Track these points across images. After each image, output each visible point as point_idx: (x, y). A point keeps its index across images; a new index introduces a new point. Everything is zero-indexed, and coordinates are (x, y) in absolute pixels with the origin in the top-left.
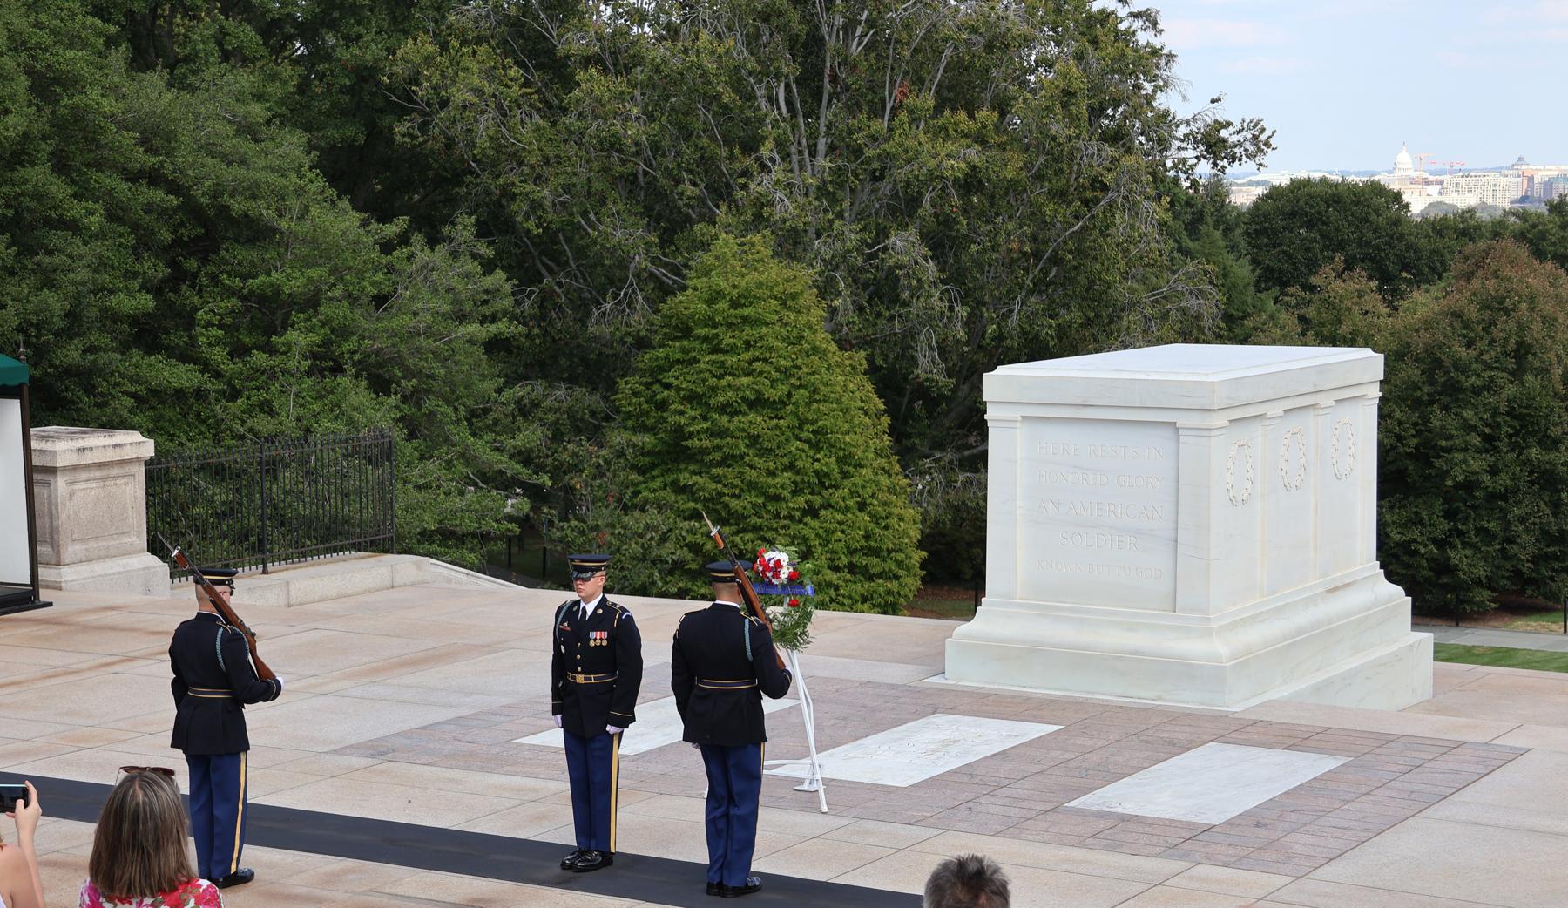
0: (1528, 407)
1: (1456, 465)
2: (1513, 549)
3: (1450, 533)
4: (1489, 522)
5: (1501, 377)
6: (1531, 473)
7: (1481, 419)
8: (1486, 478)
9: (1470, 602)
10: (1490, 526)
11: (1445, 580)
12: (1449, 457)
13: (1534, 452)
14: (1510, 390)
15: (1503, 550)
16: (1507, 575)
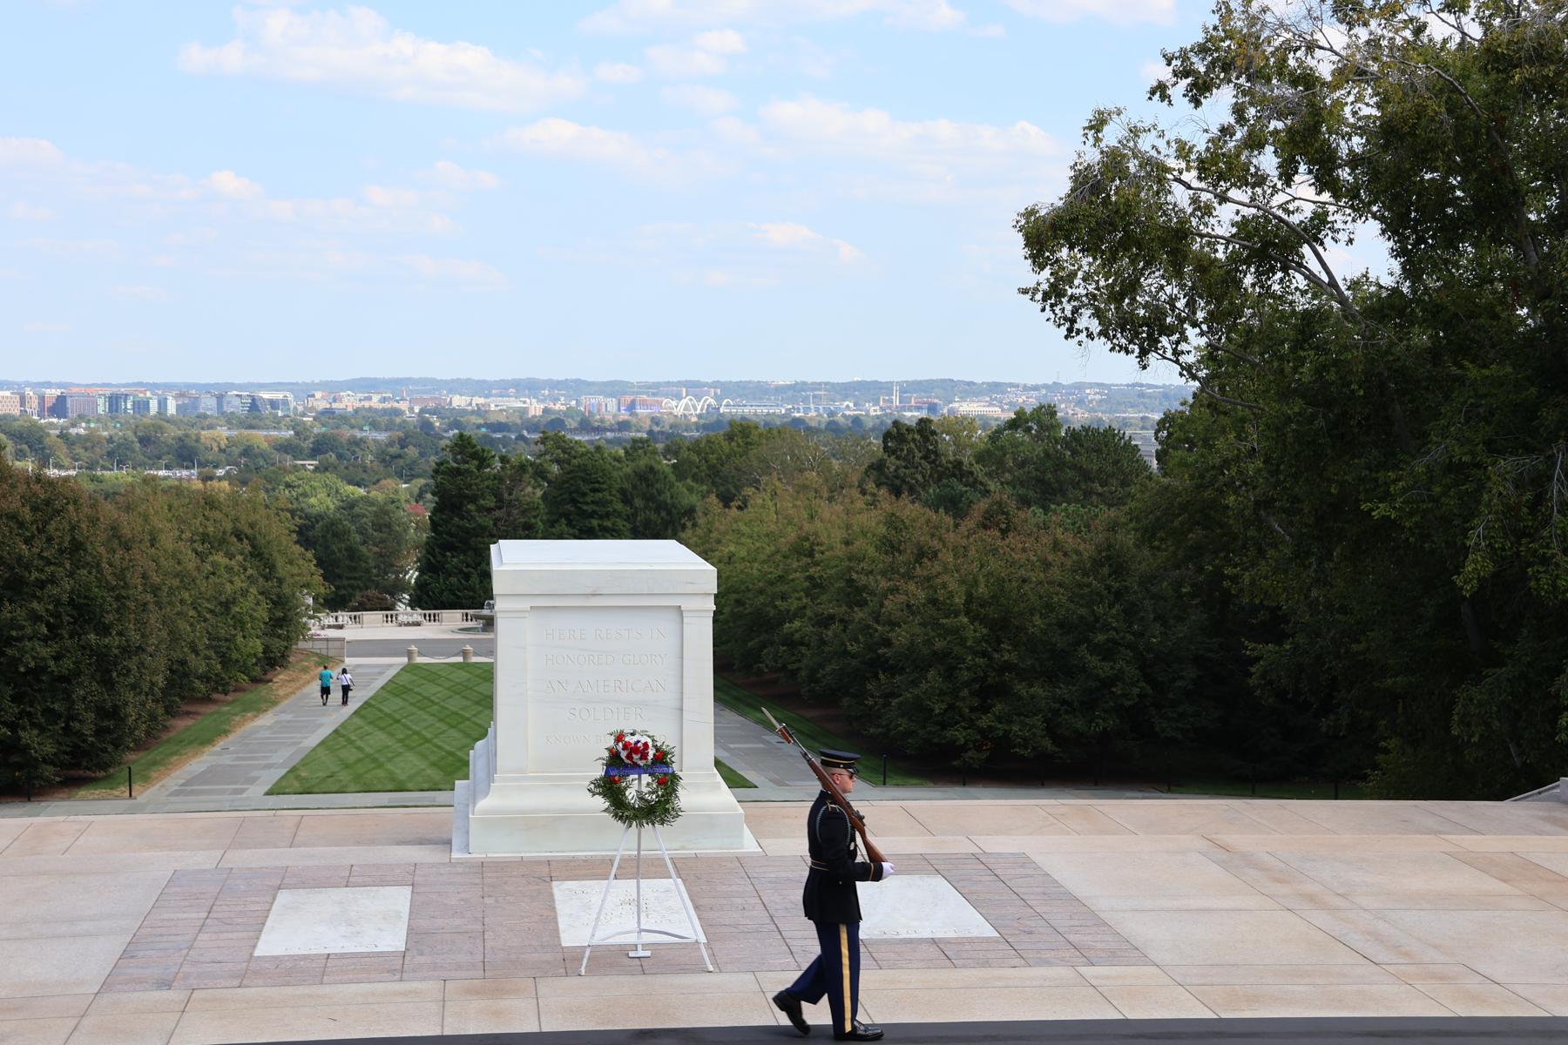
0: (86, 597)
1: (26, 652)
2: (76, 725)
3: (22, 714)
4: (53, 703)
5: (60, 572)
6: (91, 657)
7: (47, 610)
8: (52, 663)
9: (40, 777)
10: (56, 706)
11: (15, 759)
12: (20, 645)
13: (92, 636)
14: (67, 585)
15: (67, 729)
16: (68, 749)
